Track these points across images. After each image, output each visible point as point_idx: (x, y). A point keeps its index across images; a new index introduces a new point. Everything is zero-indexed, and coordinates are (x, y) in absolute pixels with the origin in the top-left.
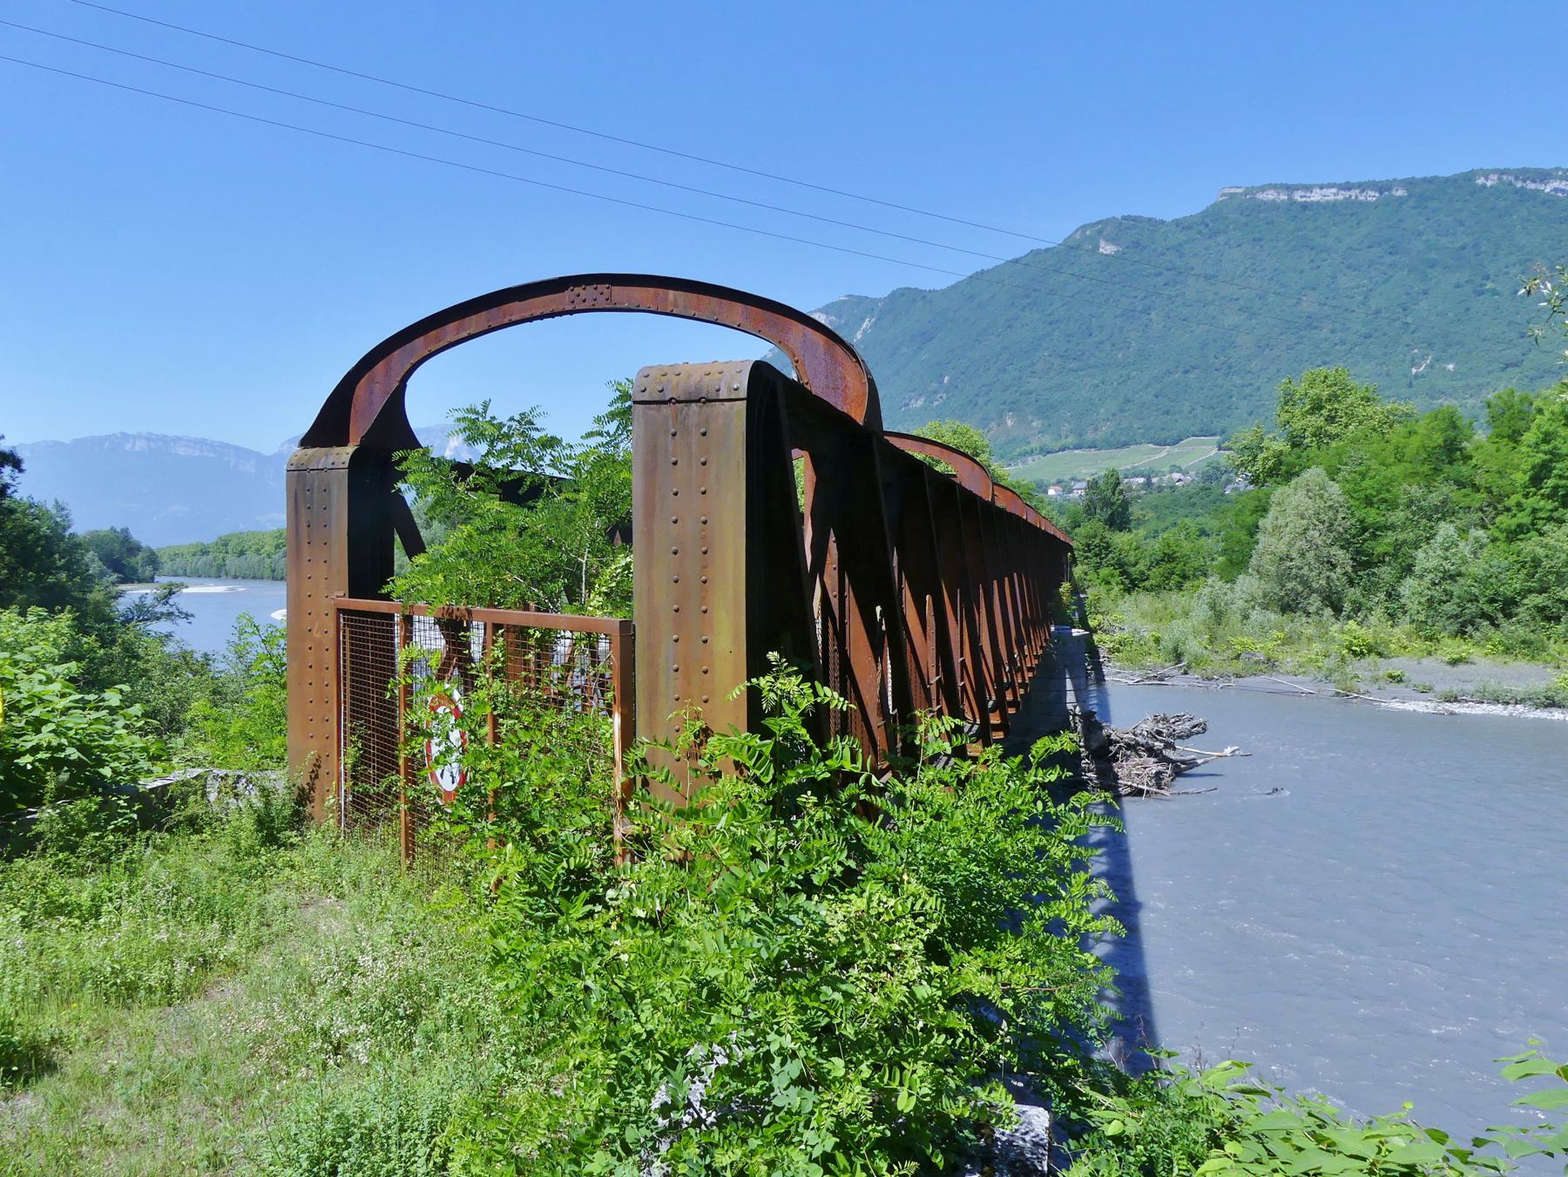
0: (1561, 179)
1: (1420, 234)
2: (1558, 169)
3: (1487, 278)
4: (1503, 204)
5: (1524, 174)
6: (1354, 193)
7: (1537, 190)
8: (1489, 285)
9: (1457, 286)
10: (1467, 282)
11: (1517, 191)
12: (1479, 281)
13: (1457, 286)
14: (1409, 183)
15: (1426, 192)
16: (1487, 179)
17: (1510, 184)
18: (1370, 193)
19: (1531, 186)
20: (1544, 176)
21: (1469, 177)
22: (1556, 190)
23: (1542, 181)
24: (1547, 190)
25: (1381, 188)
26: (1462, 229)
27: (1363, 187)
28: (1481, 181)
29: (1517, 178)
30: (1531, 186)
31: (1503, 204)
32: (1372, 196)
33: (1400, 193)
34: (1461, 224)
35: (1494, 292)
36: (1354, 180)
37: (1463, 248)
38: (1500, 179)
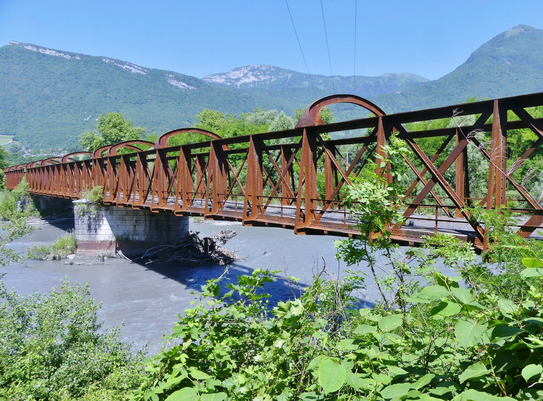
0: (128, 65)
1: (86, 74)
2: (127, 62)
3: (107, 92)
4: (111, 69)
5: (117, 61)
6: (62, 55)
7: (121, 67)
8: (108, 95)
9: (98, 93)
10: (101, 92)
11: (115, 66)
12: (105, 93)
13: (98, 93)
14: (82, 56)
15: (87, 60)
16: (106, 60)
17: (113, 63)
18: (68, 56)
19: (119, 65)
20: (123, 63)
21: (101, 58)
22: (126, 68)
23: (122, 65)
24: (124, 68)
25: (72, 55)
26: (99, 75)
27: (65, 53)
28: (104, 60)
29: (115, 62)
30: (119, 65)
31: (111, 69)
32: (68, 57)
33: (78, 58)
34: (99, 73)
35: (110, 97)
36: (62, 50)
37: (99, 81)
38: (110, 61)
